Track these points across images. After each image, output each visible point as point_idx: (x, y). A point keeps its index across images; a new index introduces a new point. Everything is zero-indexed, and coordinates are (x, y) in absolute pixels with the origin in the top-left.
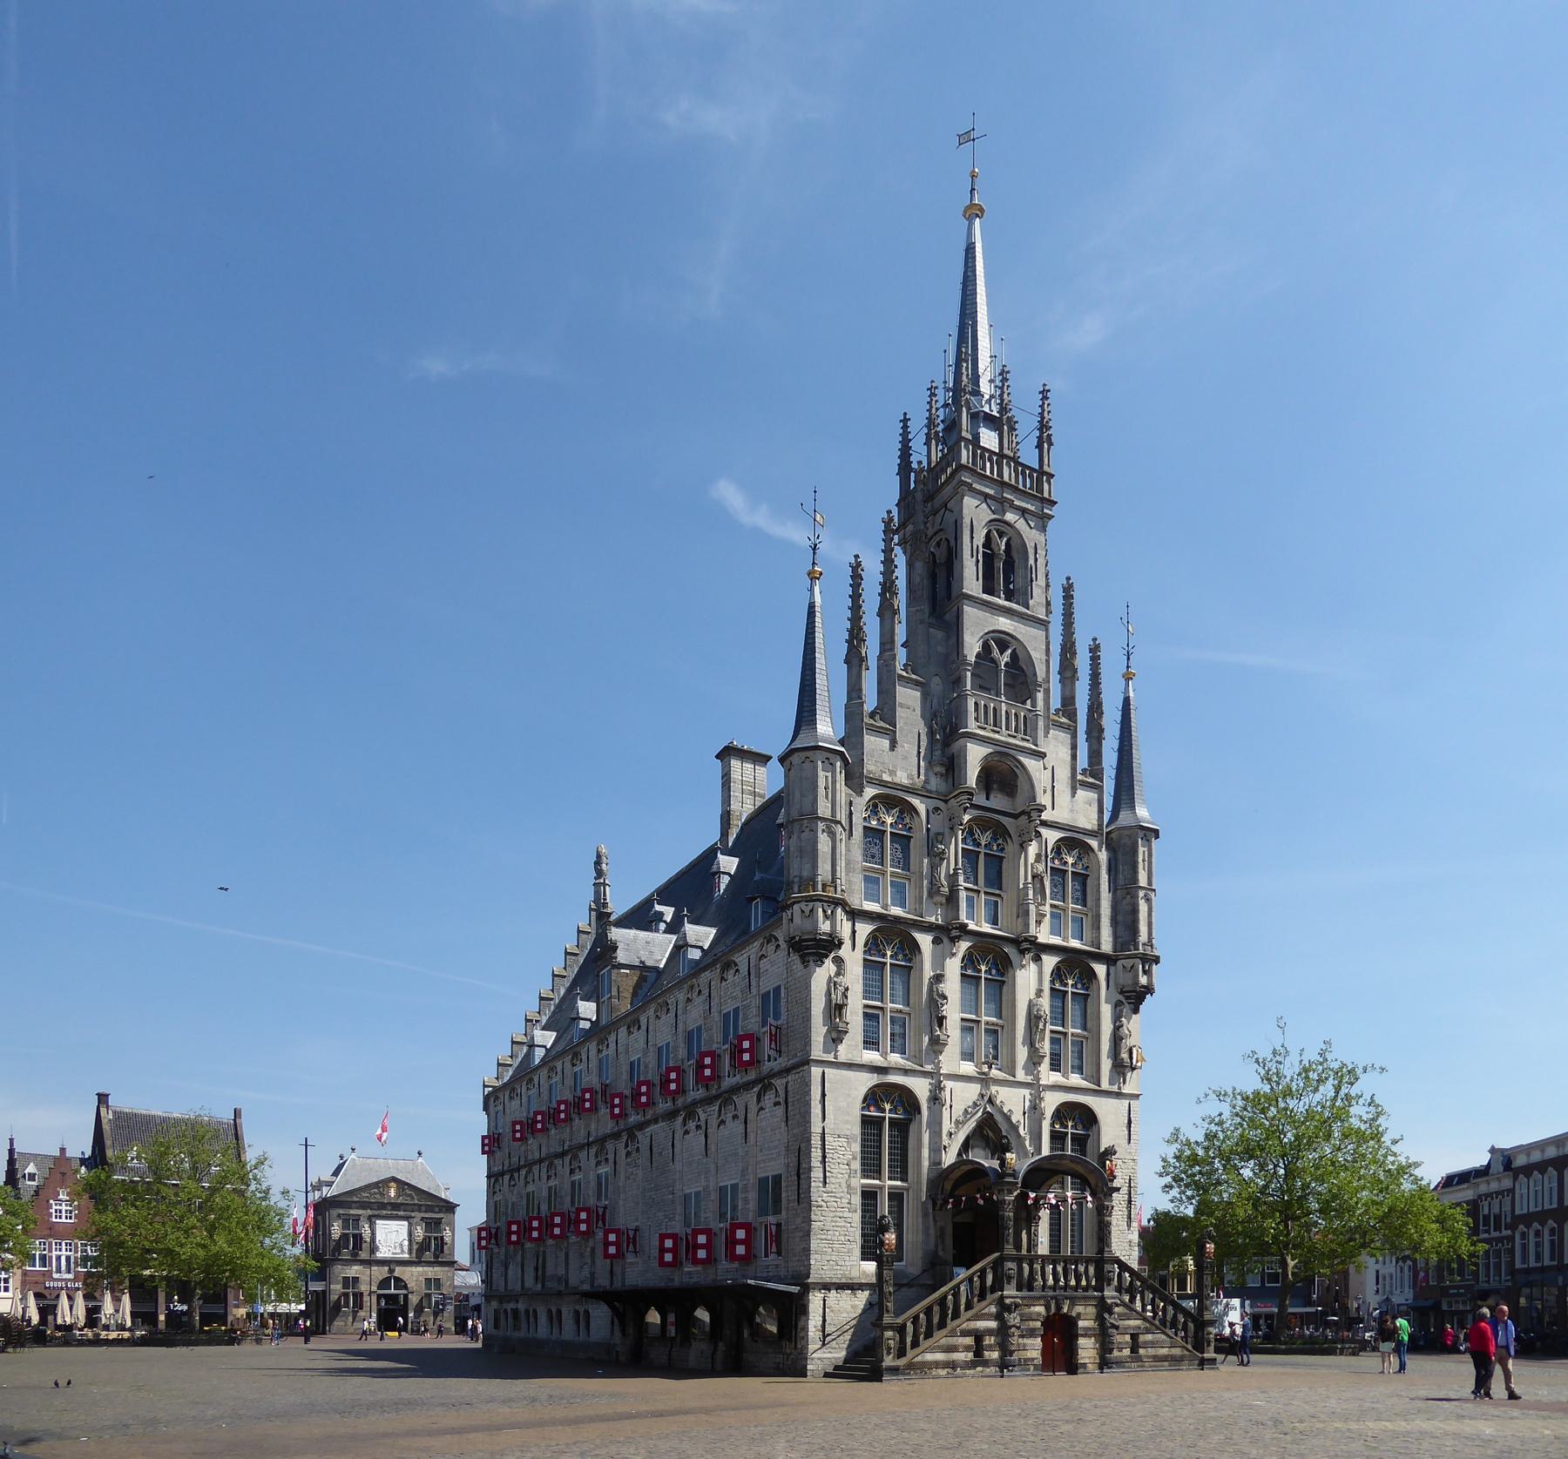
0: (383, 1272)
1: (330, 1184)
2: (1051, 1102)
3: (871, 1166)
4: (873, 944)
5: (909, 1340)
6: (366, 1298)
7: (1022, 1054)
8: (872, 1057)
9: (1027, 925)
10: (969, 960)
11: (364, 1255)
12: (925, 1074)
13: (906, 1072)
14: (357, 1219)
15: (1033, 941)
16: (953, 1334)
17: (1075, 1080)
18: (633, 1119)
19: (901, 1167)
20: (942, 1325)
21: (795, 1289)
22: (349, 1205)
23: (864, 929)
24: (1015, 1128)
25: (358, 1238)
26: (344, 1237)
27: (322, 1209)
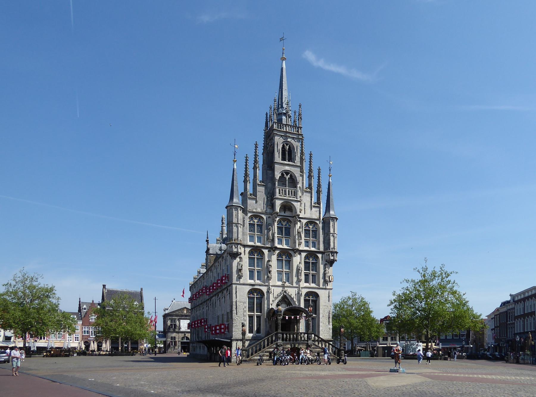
0: (183, 335)
1: (167, 309)
2: (304, 292)
3: (251, 309)
4: (251, 253)
5: (250, 353)
6: (177, 343)
7: (295, 279)
8: (252, 282)
9: (295, 246)
10: (279, 255)
11: (177, 330)
12: (265, 286)
13: (260, 285)
14: (175, 320)
15: (298, 250)
16: (263, 352)
17: (313, 285)
18: (211, 295)
19: (260, 309)
20: (260, 350)
21: (229, 341)
22: (172, 316)
23: (247, 250)
24: (293, 299)
25: (175, 325)
26: (171, 325)
27: (165, 316)
